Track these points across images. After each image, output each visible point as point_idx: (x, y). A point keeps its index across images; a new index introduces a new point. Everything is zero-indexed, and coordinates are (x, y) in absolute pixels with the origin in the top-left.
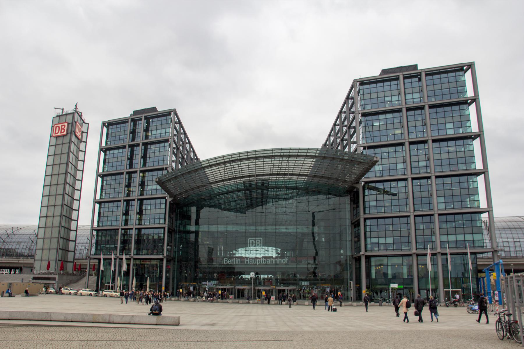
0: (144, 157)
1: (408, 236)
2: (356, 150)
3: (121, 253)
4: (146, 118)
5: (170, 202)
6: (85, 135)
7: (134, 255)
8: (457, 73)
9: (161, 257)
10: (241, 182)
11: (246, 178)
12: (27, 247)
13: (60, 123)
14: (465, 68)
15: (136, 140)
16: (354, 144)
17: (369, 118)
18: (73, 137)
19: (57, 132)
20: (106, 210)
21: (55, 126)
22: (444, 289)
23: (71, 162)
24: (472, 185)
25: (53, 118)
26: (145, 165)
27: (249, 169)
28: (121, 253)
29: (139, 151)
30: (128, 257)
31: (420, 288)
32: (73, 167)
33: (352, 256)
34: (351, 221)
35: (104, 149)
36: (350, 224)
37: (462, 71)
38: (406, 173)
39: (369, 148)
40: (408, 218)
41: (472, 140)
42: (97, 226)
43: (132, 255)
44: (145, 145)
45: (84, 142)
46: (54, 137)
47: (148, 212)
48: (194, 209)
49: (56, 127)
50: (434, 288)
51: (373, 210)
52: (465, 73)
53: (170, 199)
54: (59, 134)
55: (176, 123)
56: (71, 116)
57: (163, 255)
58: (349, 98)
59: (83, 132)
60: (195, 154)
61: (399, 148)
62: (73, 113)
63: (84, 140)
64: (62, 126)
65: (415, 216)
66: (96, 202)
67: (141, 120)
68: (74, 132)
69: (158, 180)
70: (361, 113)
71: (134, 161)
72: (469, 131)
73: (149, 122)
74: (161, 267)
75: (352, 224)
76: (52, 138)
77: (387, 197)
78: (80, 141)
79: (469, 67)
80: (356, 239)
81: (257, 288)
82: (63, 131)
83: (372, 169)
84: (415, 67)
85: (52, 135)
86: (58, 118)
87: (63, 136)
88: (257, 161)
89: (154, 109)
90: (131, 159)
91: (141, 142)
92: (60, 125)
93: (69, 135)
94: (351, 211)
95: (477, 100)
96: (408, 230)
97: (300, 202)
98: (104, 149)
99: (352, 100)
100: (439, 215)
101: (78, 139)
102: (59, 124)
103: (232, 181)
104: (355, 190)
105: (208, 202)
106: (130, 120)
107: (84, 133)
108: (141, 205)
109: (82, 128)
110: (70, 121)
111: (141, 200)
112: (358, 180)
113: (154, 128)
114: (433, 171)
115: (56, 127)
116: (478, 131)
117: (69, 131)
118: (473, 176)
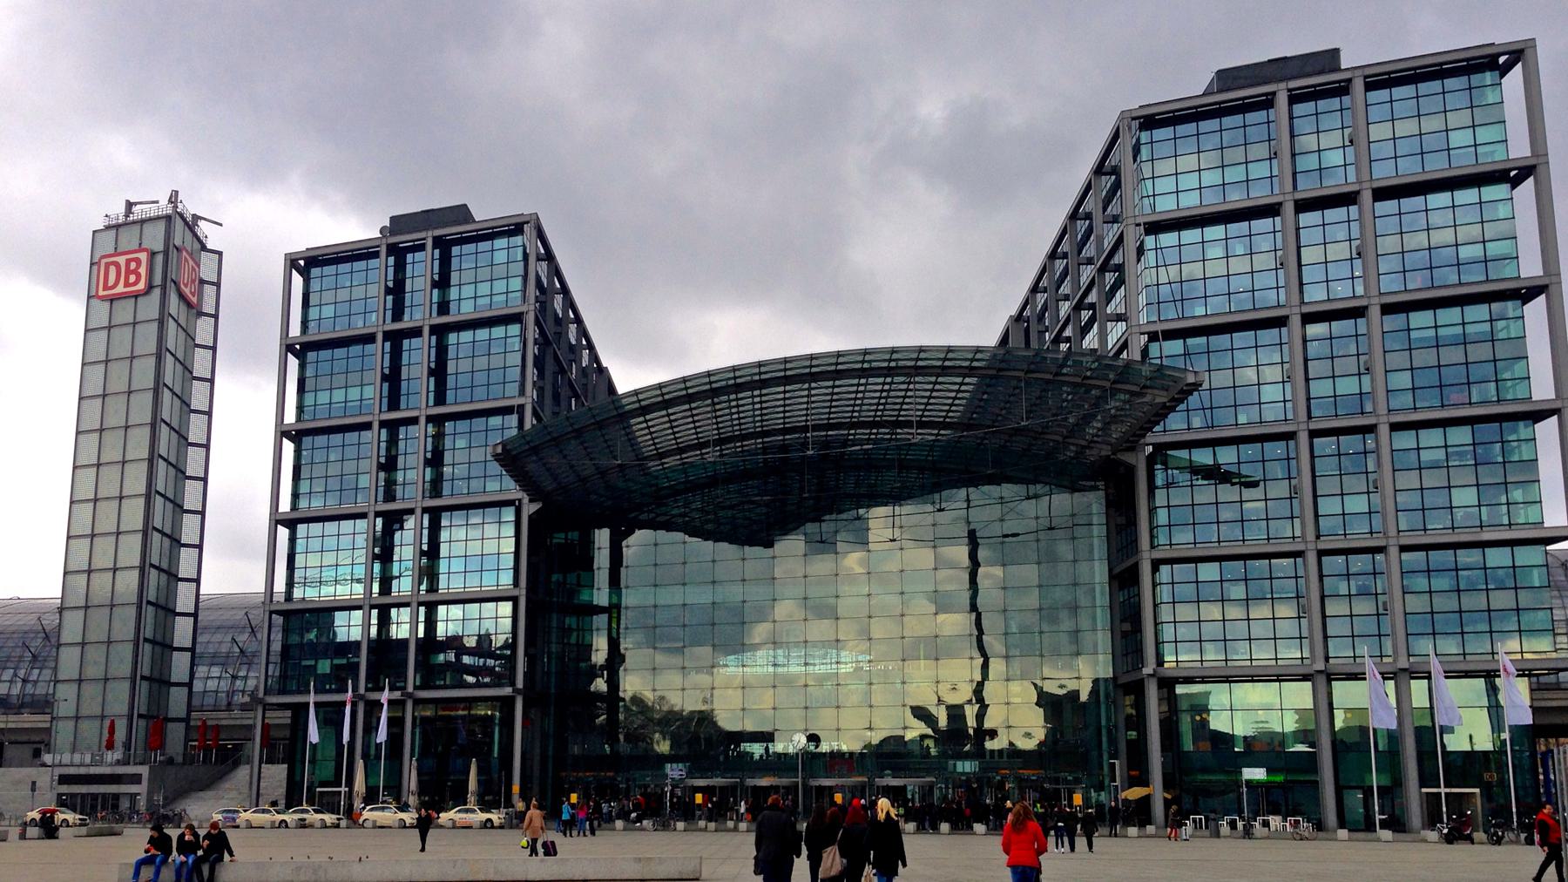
0: (439, 372)
1: (1299, 617)
2: (1125, 346)
3: (370, 686)
4: (438, 242)
5: (530, 517)
6: (209, 291)
7: (416, 688)
8: (1476, 79)
9: (508, 691)
10: (757, 449)
11: (774, 435)
12: (15, 675)
14: (1502, 60)
15: (406, 317)
16: (1117, 321)
17: (1168, 239)
18: (173, 299)
19: (111, 282)
20: (315, 544)
21: (104, 261)
22: (1421, 786)
23: (171, 387)
24: (1517, 451)
25: (94, 232)
26: (440, 399)
27: (787, 408)
28: (370, 686)
29: (418, 354)
30: (397, 695)
31: (1342, 783)
32: (177, 402)
33: (1115, 678)
34: (1110, 570)
35: (298, 347)
36: (1106, 578)
37: (1491, 70)
38: (1290, 416)
39: (1170, 335)
40: (1299, 560)
41: (1519, 302)
42: (286, 600)
43: (410, 689)
44: (440, 331)
47: (458, 549)
48: (602, 537)
49: (108, 265)
50: (1386, 782)
51: (1183, 536)
52: (1502, 75)
53: (535, 507)
54: (120, 289)
55: (539, 259)
56: (161, 227)
57: (513, 684)
58: (1104, 170)
59: (202, 282)
60: (595, 358)
61: (1269, 335)
62: (168, 218)
63: (208, 307)
64: (128, 262)
65: (1321, 553)
66: (278, 522)
67: (422, 248)
68: (175, 283)
69: (499, 450)
70: (1145, 224)
71: (404, 385)
72: (1509, 272)
73: (450, 257)
74: (508, 723)
75: (1112, 577)
76: (94, 302)
77: (1228, 492)
78: (195, 311)
79: (1516, 55)
80: (1127, 627)
81: (815, 783)
82: (132, 278)
83: (1182, 407)
84: (1330, 58)
86: (113, 232)
87: (136, 296)
88: (813, 385)
89: (461, 213)
90: (393, 378)
91: (427, 322)
92: (122, 260)
93: (157, 292)
94: (1108, 537)
95: (1540, 169)
96: (1298, 597)
97: (943, 510)
98: (298, 347)
99: (1113, 177)
100: (1404, 549)
101: (189, 305)
102: (116, 254)
103: (728, 446)
104: (1122, 470)
105: (651, 511)
106: (383, 250)
107: (206, 286)
108: (435, 529)
109: (199, 266)
110: (159, 246)
111: (435, 515)
112: (1132, 442)
113: (468, 276)
114: (1383, 410)
115: (108, 265)
116: (1541, 274)
117: (158, 280)
118: (1521, 424)
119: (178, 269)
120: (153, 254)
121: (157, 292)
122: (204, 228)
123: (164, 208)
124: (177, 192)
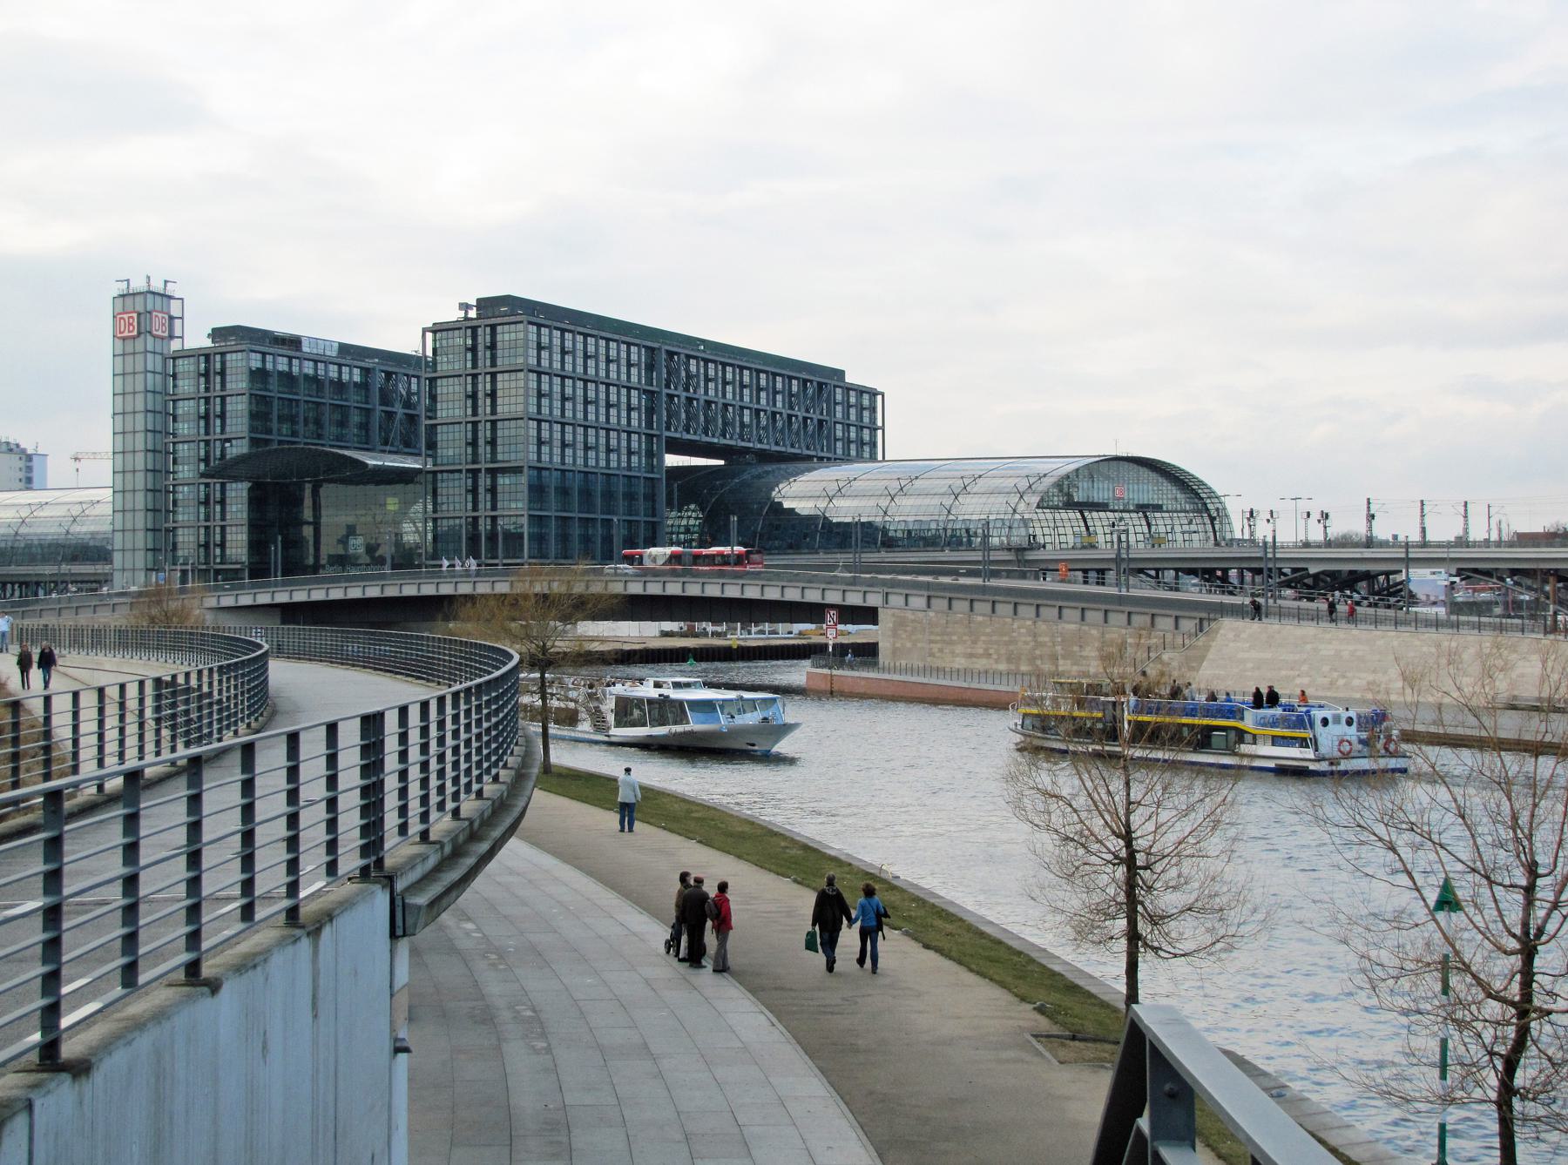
6: (177, 323)
7: (215, 563)
45: (178, 337)
49: (121, 318)
54: (126, 334)
59: (171, 318)
63: (177, 333)
64: (129, 318)
68: (150, 332)
82: (131, 328)
86: (121, 299)
87: (134, 338)
92: (126, 316)
93: (142, 336)
101: (162, 338)
119: (151, 323)
122: (171, 290)
124: (148, 278)
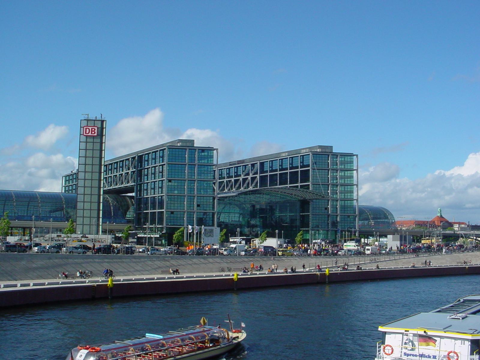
13: (88, 126)
19: (87, 132)
21: (85, 127)
25: (81, 120)
46: (85, 135)
49: (86, 129)
54: (90, 134)
56: (100, 122)
64: (92, 129)
82: (93, 132)
85: (82, 133)
86: (86, 122)
87: (94, 137)
92: (90, 128)
110: (100, 126)
117: (99, 134)
120: (99, 128)
121: (99, 137)
123: (99, 118)
